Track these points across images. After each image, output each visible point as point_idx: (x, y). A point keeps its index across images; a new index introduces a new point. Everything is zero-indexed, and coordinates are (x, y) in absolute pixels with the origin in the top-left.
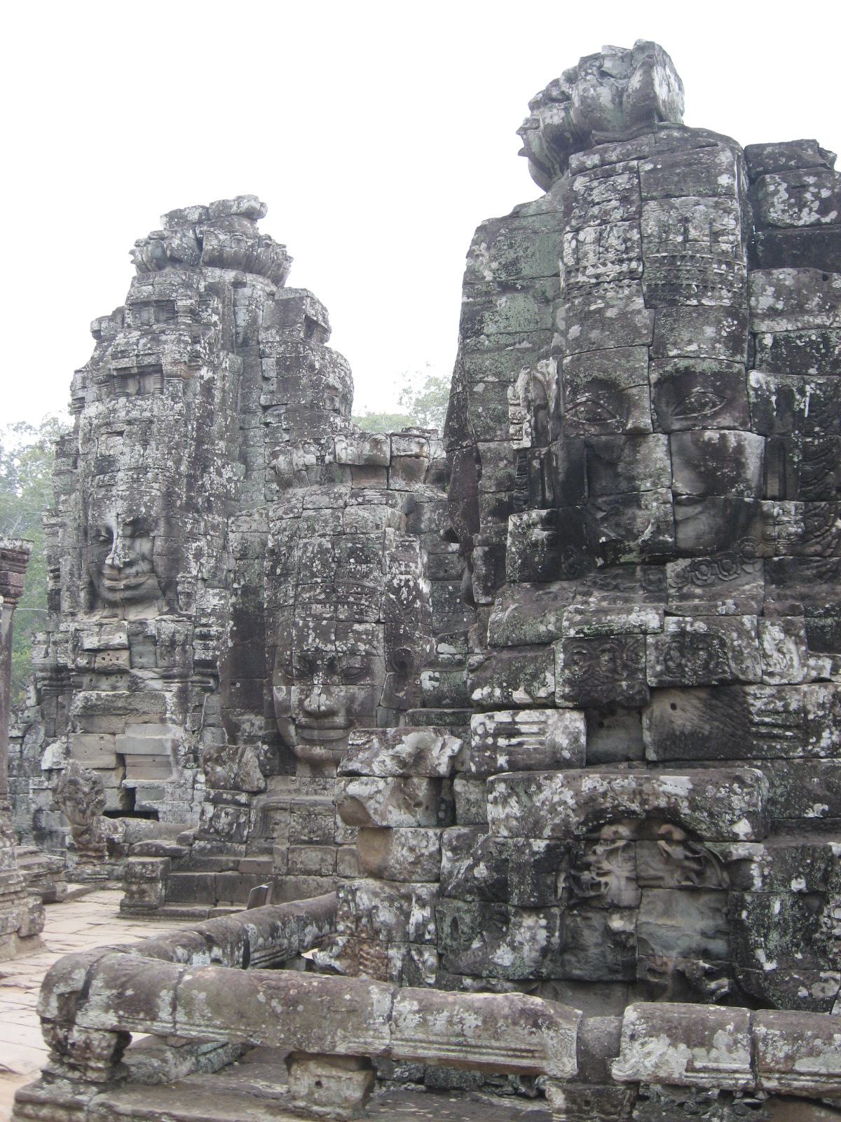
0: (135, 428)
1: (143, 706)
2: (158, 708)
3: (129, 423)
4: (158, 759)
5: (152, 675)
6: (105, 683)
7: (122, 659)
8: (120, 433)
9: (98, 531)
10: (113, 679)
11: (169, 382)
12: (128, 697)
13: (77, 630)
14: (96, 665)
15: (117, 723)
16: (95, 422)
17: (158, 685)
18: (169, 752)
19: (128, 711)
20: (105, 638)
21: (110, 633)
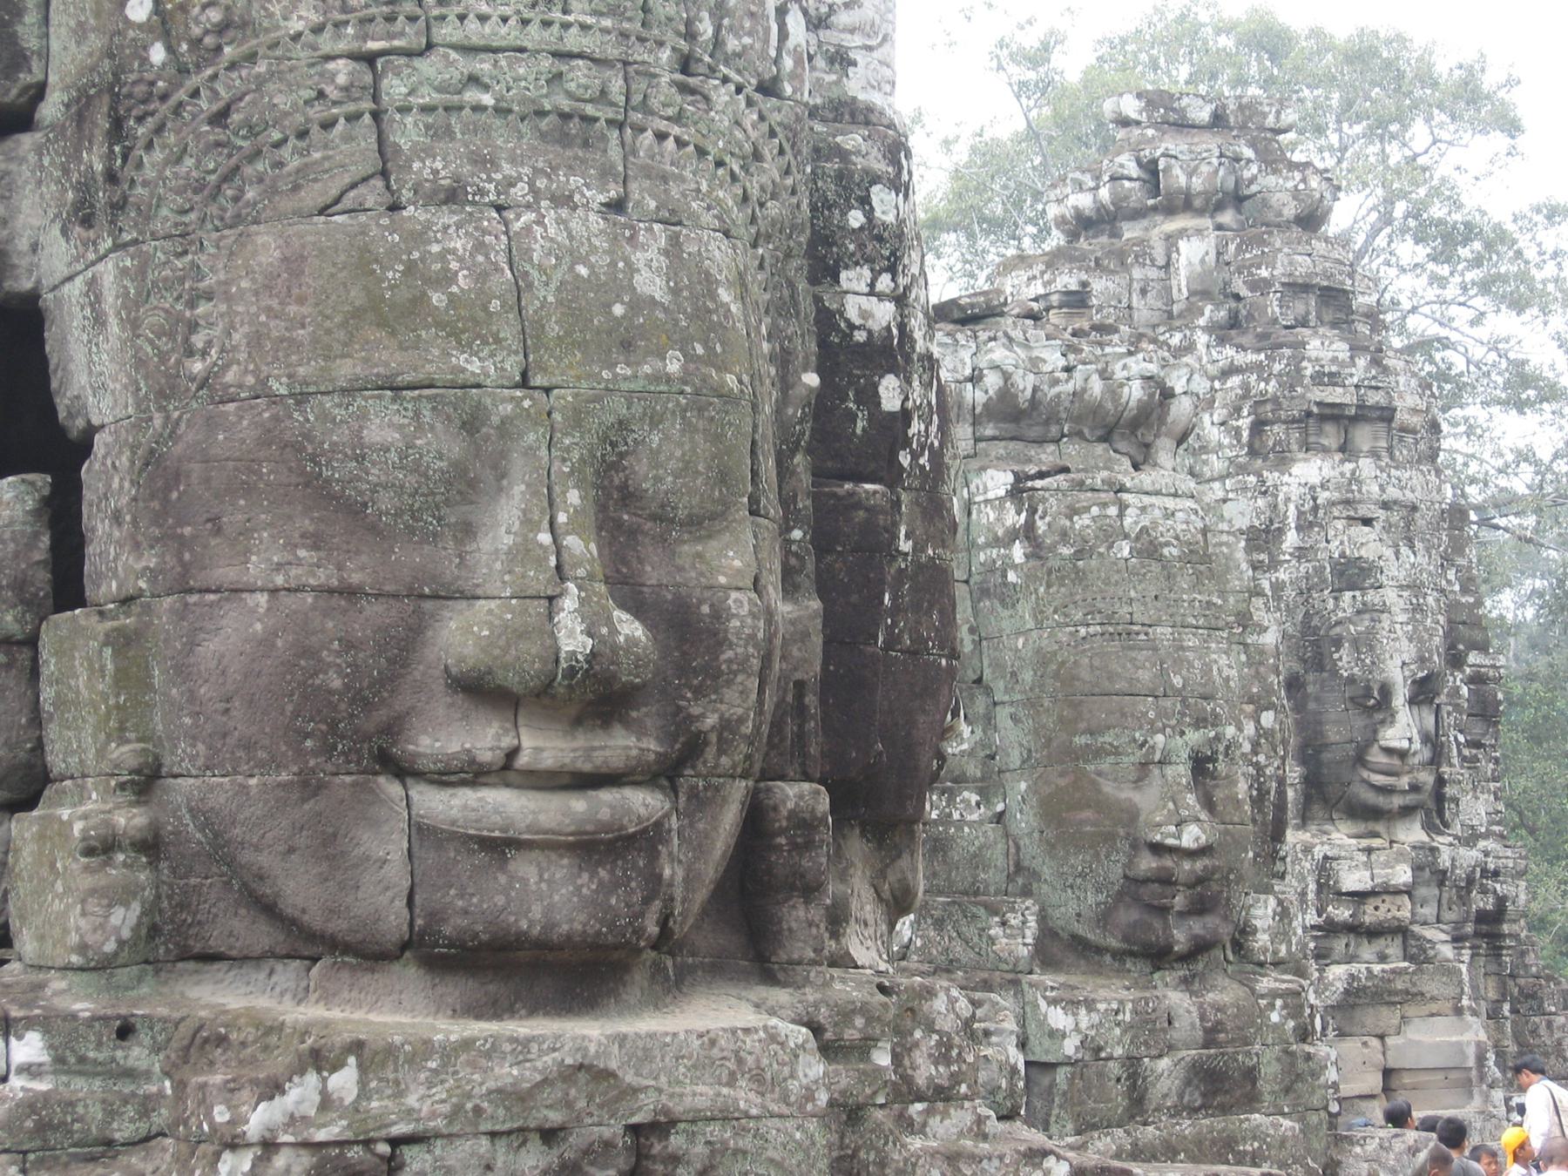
0: (1395, 517)
1: (1431, 986)
2: (1451, 991)
3: (1385, 505)
4: (1453, 1075)
5: (1444, 937)
6: (1367, 951)
7: (1403, 910)
8: (1367, 522)
9: (1368, 693)
10: (1380, 944)
11: (1401, 439)
12: (1414, 973)
13: (1326, 858)
14: (1367, 919)
15: (1388, 1017)
16: (1323, 496)
17: (1447, 951)
18: (1471, 1062)
19: (1413, 996)
20: (1382, 874)
21: (1387, 865)
